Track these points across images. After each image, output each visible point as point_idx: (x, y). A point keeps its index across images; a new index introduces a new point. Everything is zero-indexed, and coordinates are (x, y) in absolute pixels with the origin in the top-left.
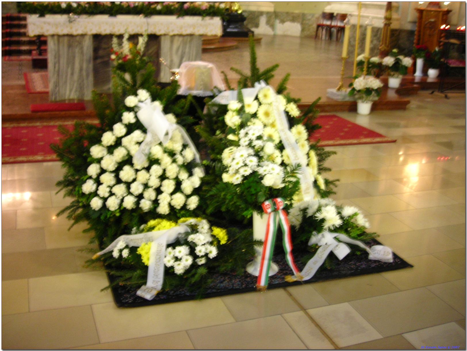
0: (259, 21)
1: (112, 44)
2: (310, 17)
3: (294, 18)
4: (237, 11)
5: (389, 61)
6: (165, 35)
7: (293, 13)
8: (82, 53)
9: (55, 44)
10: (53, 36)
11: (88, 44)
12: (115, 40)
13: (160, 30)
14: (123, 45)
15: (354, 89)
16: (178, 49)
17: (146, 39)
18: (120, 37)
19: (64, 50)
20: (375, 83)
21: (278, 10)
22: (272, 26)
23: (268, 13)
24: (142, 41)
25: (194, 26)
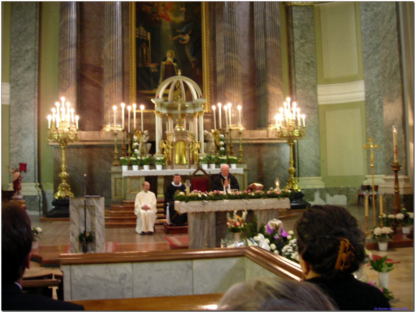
0: (314, 196)
1: (226, 216)
2: (352, 190)
3: (340, 192)
4: (297, 190)
5: (400, 216)
6: (257, 210)
7: (339, 188)
8: (209, 223)
9: (194, 217)
10: (193, 213)
11: (212, 217)
12: (228, 214)
13: (254, 207)
14: (234, 216)
15: (375, 235)
16: (265, 217)
17: (246, 213)
18: (232, 213)
19: (199, 221)
20: (387, 230)
21: (328, 186)
22: (324, 199)
23: (320, 190)
24: (244, 214)
25: (273, 204)
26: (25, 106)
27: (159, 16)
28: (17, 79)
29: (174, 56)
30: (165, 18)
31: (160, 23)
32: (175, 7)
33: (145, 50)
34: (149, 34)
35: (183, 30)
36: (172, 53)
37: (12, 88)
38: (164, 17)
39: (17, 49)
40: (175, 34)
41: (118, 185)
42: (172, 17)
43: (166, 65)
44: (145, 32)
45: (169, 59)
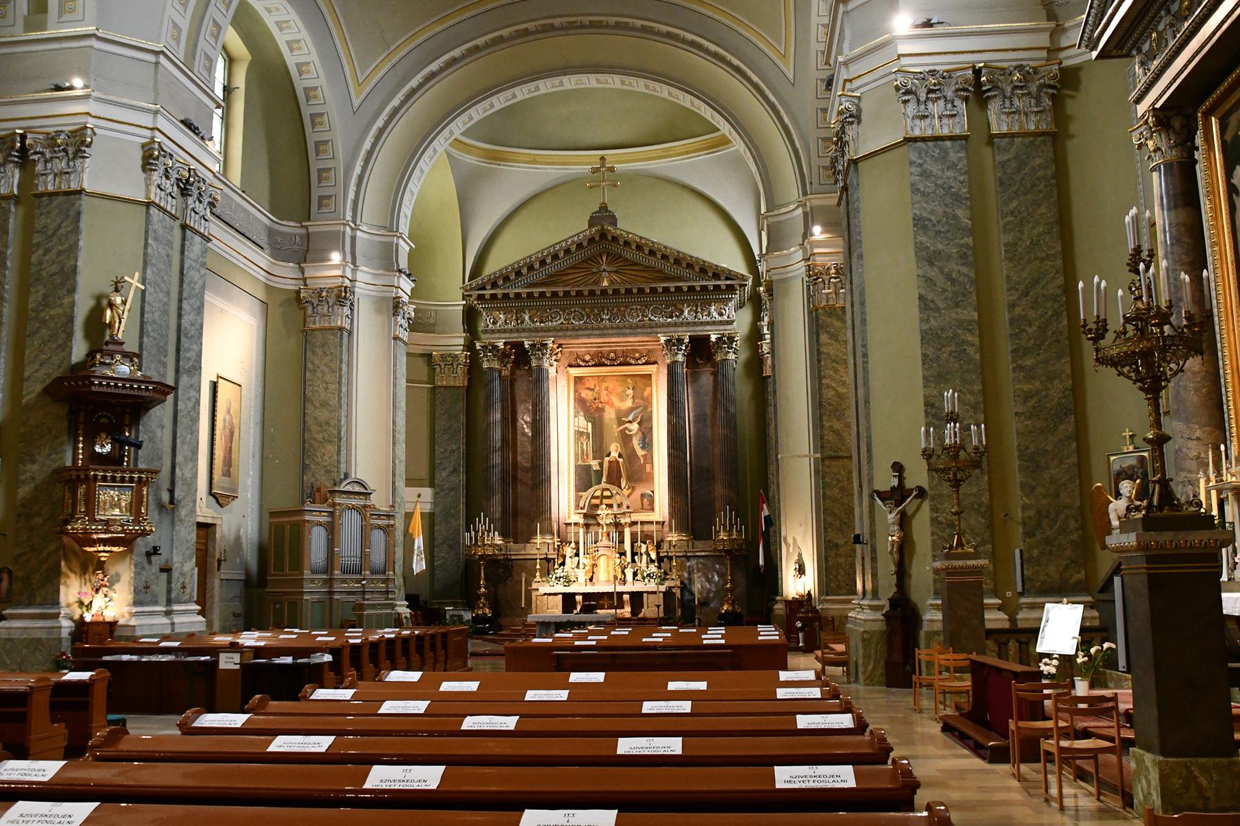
29: (619, 450)
31: (602, 410)
33: (585, 444)
34: (590, 425)
35: (630, 418)
38: (608, 404)
40: (621, 423)
41: (538, 602)
42: (617, 403)
45: (614, 454)
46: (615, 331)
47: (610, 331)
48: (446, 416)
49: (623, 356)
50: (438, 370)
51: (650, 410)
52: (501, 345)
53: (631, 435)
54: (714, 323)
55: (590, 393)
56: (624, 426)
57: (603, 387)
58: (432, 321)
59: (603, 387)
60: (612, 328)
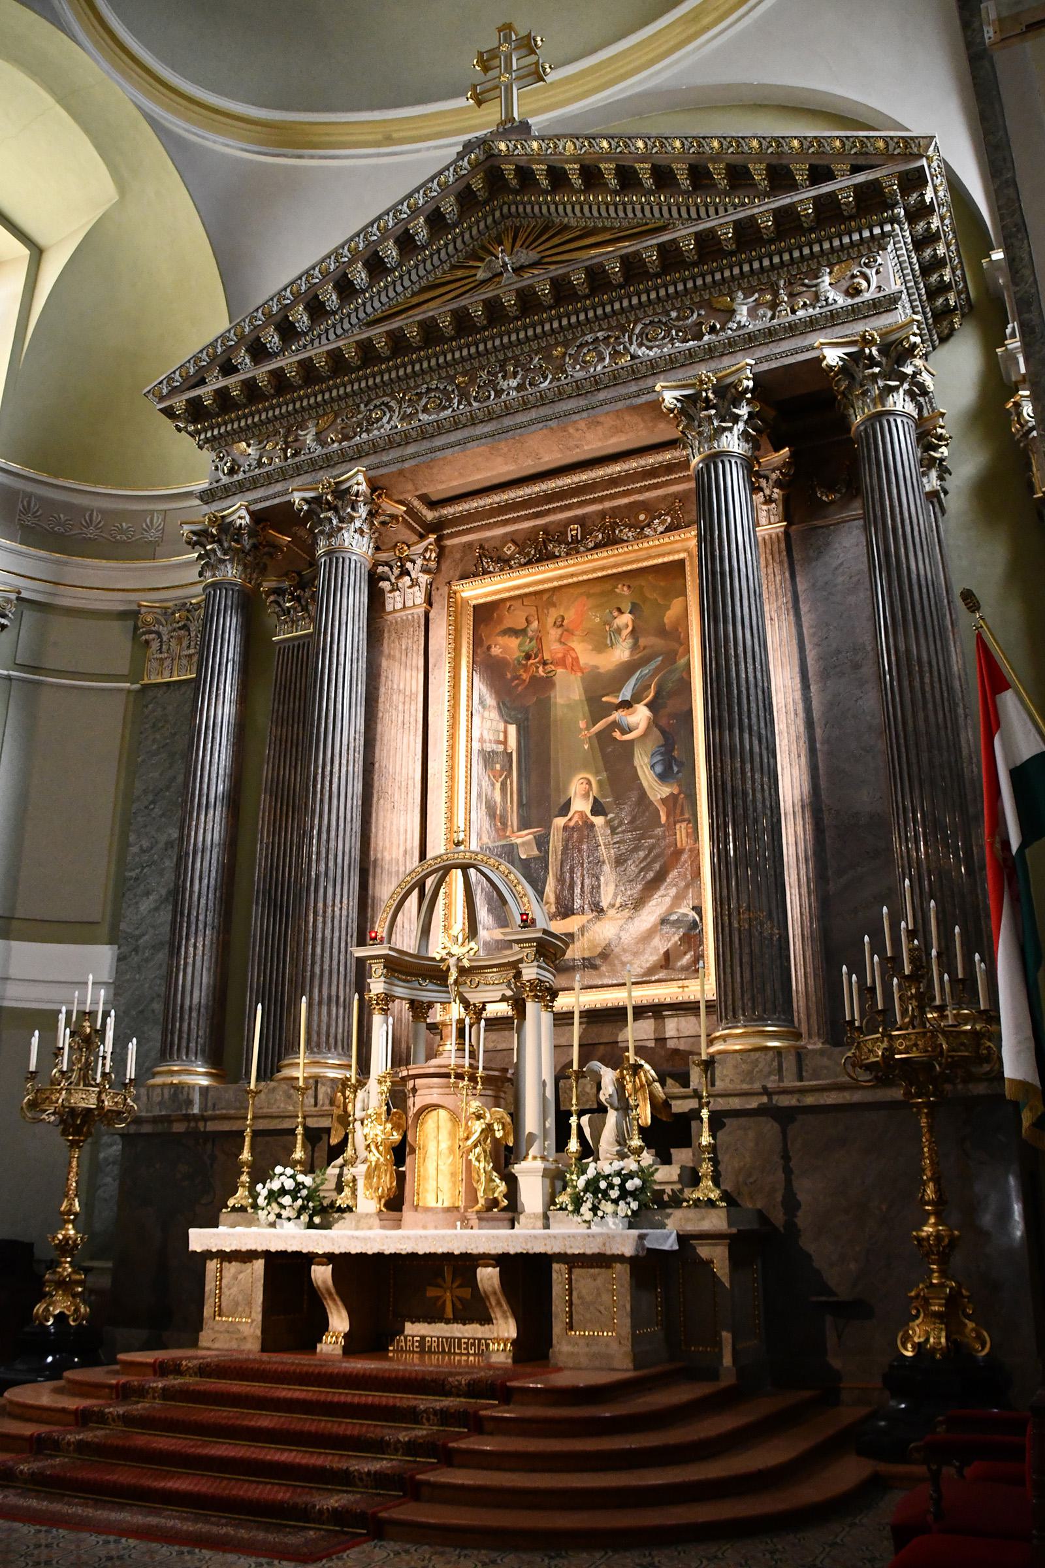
26: (153, 1011)
27: (545, 663)
28: (137, 932)
30: (565, 666)
31: (548, 683)
32: (598, 620)
34: (512, 729)
35: (626, 693)
36: (589, 783)
37: (121, 959)
38: (562, 662)
39: (145, 844)
42: (586, 656)
43: (565, 828)
44: (501, 726)
45: (581, 806)
46: (533, 414)
47: (521, 418)
48: (164, 755)
49: (602, 529)
50: (155, 645)
51: (683, 661)
52: (242, 518)
53: (632, 741)
54: (833, 319)
55: (513, 643)
56: (611, 718)
57: (550, 621)
58: (152, 535)
59: (550, 621)
60: (526, 406)
